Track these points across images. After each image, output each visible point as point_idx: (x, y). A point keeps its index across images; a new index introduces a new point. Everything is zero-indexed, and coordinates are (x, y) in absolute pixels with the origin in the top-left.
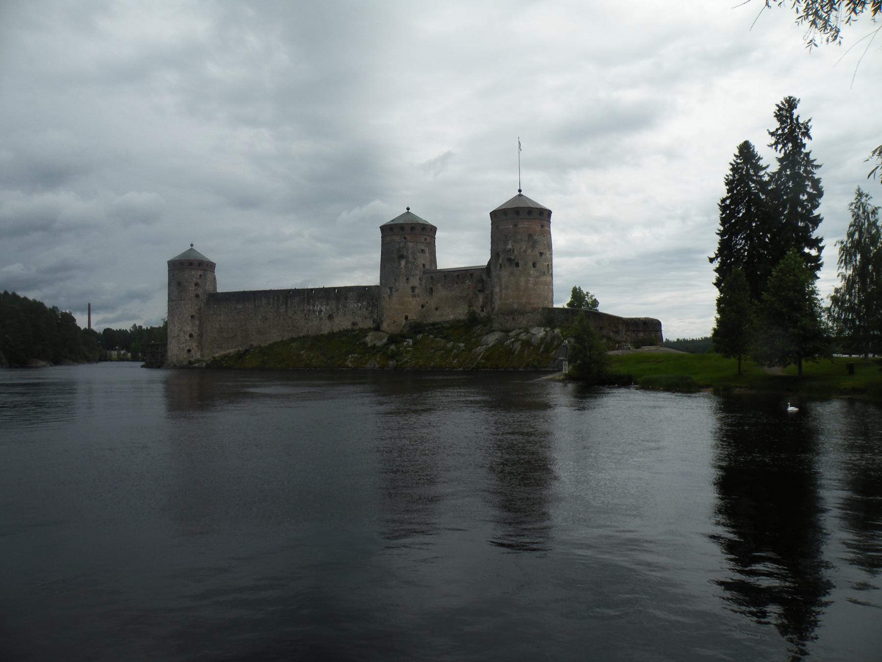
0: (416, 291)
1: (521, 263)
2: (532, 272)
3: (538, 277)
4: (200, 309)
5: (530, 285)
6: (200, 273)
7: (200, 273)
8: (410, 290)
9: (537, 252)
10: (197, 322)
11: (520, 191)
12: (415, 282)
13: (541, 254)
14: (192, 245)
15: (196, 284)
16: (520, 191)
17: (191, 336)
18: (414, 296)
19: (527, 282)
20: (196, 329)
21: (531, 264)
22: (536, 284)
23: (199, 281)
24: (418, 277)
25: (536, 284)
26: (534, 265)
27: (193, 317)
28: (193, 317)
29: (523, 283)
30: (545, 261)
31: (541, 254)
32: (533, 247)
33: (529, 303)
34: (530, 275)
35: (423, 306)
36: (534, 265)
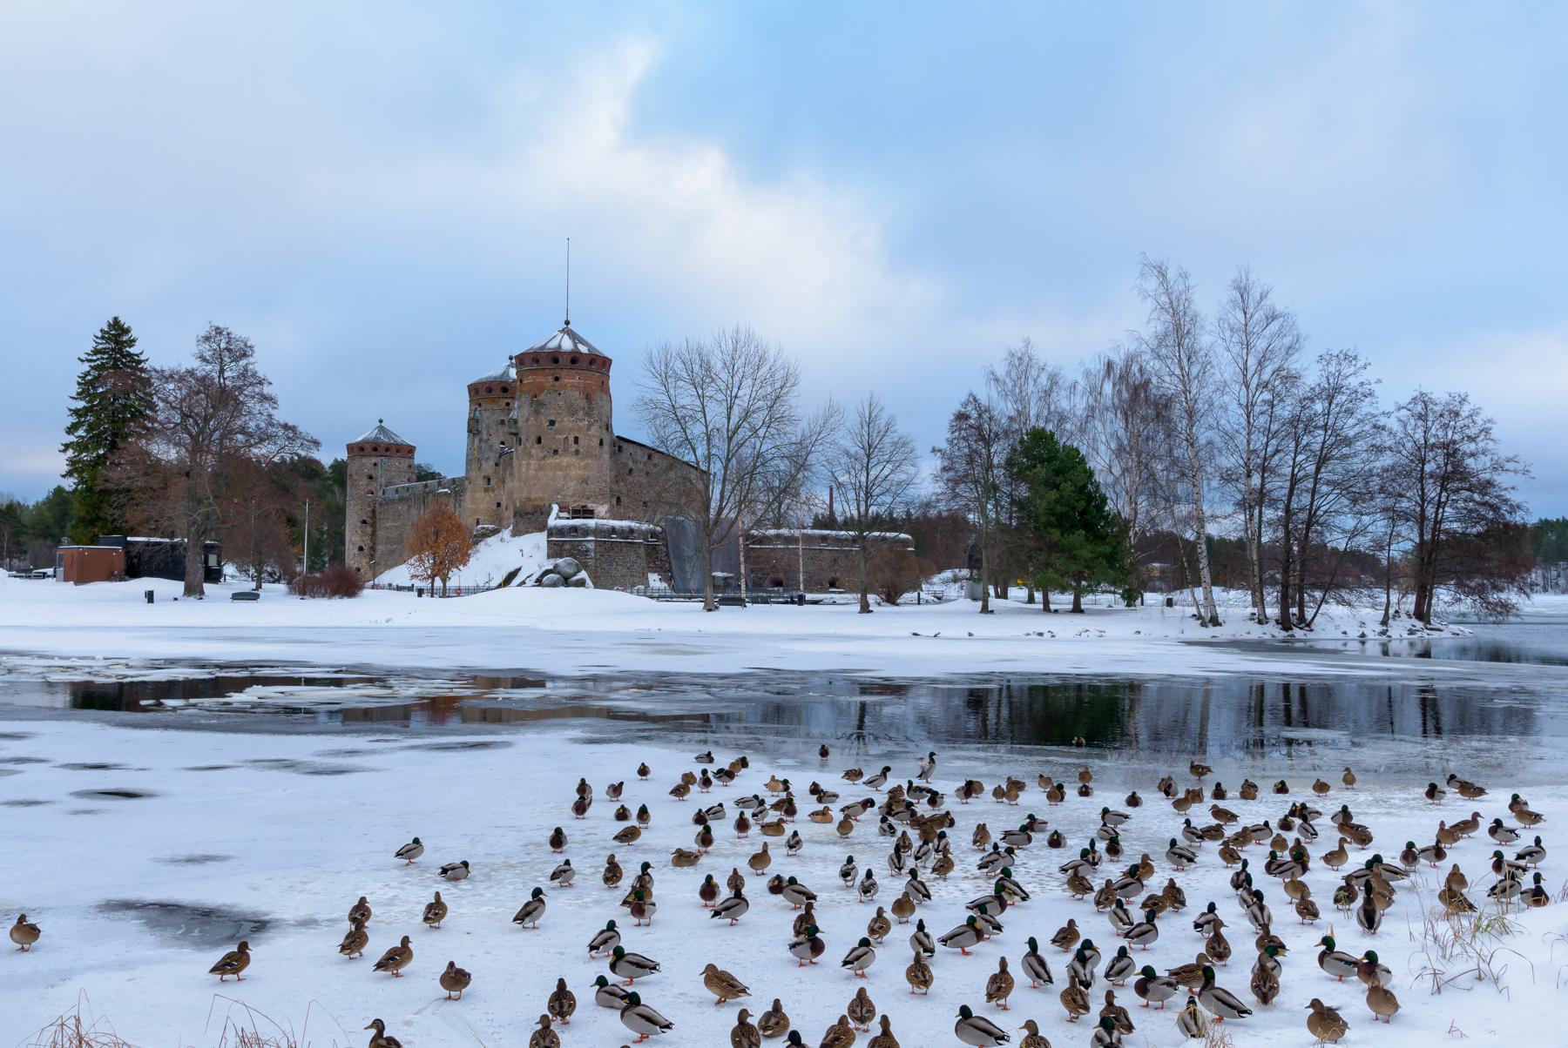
0: (493, 482)
4: (374, 511)
5: (532, 472)
7: (374, 460)
8: (481, 482)
10: (369, 530)
11: (567, 323)
12: (488, 467)
13: (552, 423)
16: (567, 323)
17: (361, 549)
18: (486, 490)
21: (534, 438)
22: (540, 468)
23: (372, 472)
24: (492, 463)
25: (540, 468)
26: (539, 441)
30: (558, 432)
31: (552, 423)
32: (537, 412)
33: (529, 499)
34: (530, 456)
35: (499, 505)
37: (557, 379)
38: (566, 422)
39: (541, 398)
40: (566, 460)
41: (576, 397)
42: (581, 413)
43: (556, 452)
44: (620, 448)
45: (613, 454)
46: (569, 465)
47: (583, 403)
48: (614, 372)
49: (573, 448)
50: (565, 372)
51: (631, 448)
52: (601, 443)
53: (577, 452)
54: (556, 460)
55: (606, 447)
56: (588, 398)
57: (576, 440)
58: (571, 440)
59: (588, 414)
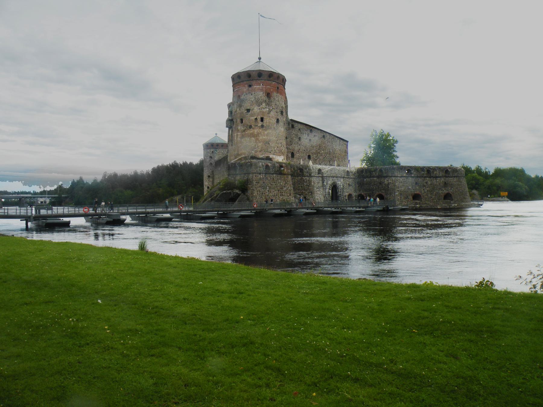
1: (235, 121)
2: (239, 128)
3: (244, 131)
4: (213, 172)
5: (239, 139)
6: (212, 150)
7: (212, 150)
9: (243, 110)
10: (211, 180)
11: (260, 59)
14: (216, 134)
15: (211, 157)
16: (260, 59)
19: (237, 135)
20: (211, 183)
21: (239, 120)
26: (242, 121)
27: (209, 176)
28: (209, 176)
29: (235, 138)
31: (248, 110)
34: (238, 130)
36: (242, 121)
37: (250, 86)
38: (256, 109)
39: (242, 97)
40: (256, 131)
41: (261, 95)
42: (264, 104)
43: (250, 127)
44: (293, 126)
45: (288, 129)
46: (258, 134)
47: (265, 98)
48: (289, 88)
49: (260, 124)
50: (254, 82)
51: (300, 126)
52: (278, 121)
53: (262, 126)
54: (251, 131)
55: (281, 123)
56: (268, 95)
57: (262, 120)
58: (259, 119)
59: (268, 104)
